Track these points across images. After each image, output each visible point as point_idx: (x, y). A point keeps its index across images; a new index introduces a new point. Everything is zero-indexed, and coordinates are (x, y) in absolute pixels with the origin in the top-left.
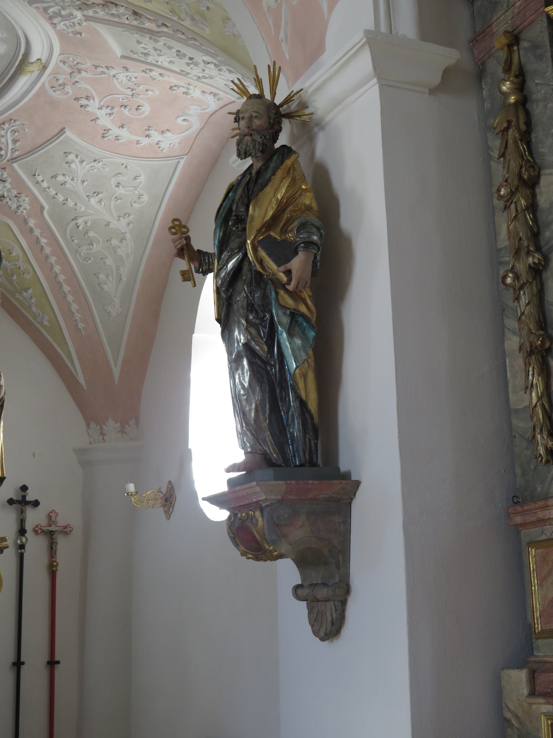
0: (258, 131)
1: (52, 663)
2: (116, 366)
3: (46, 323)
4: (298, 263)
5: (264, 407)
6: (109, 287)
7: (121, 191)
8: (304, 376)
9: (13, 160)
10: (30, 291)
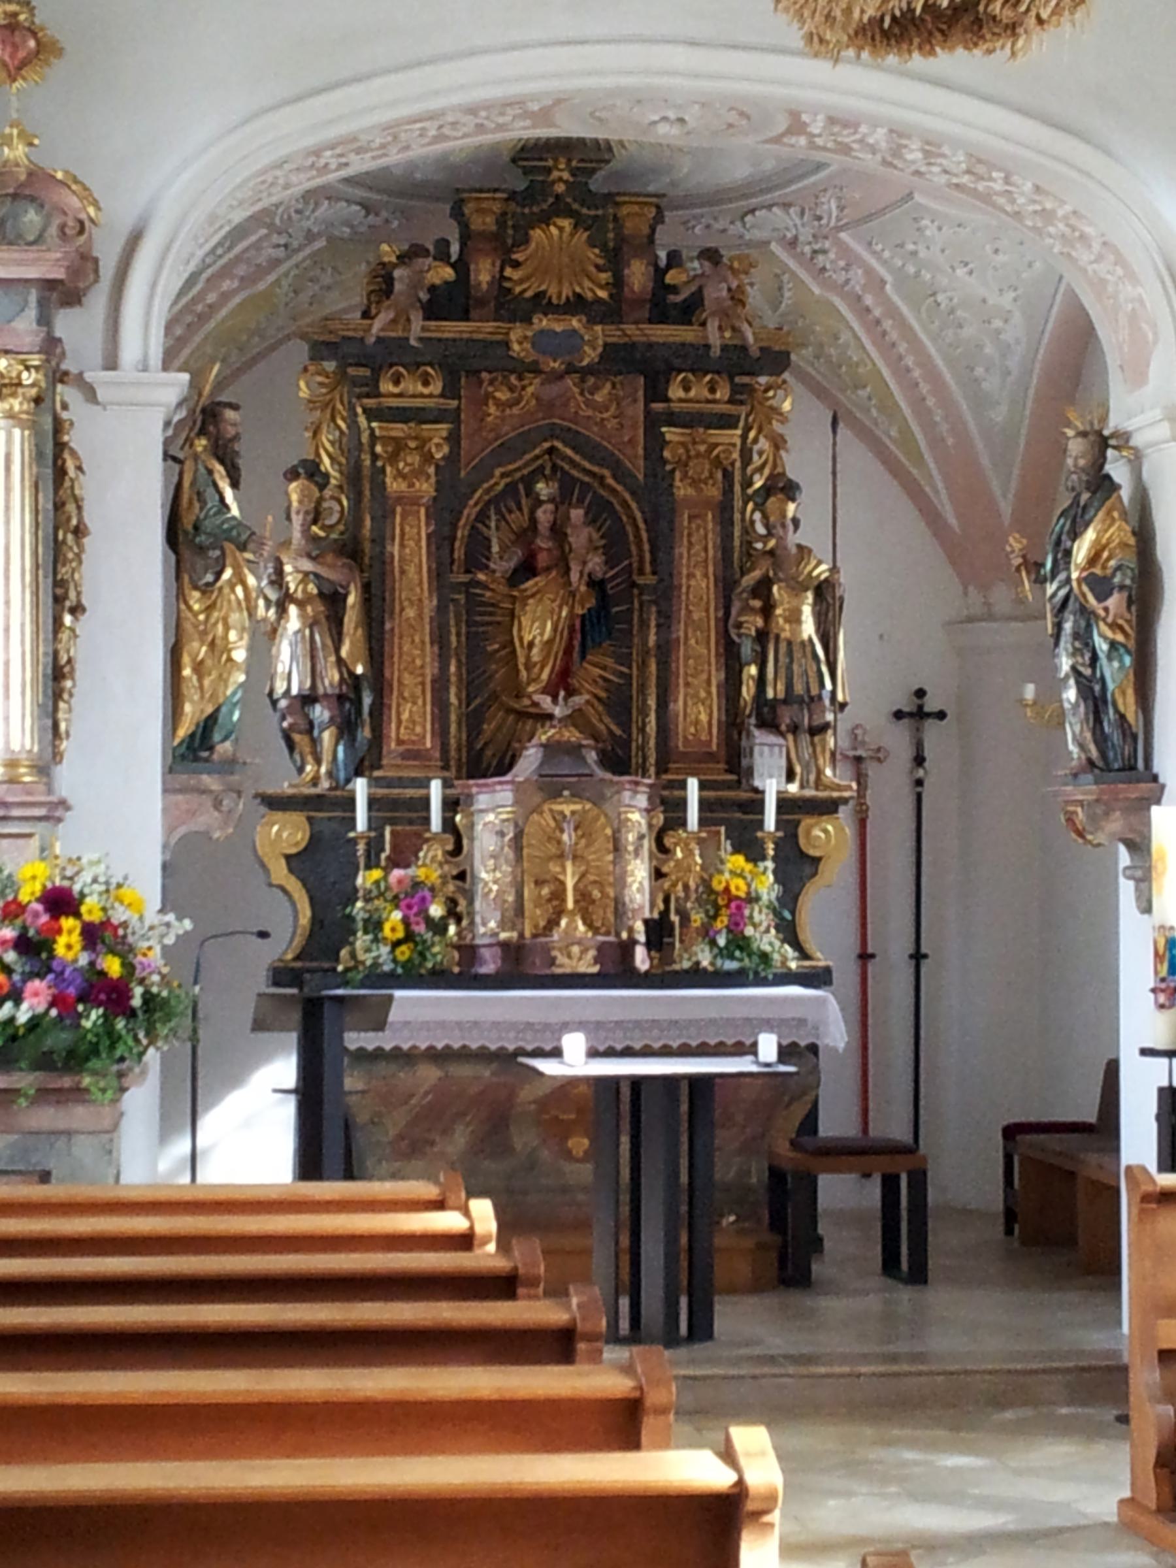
0: (1083, 470)
1: (918, 957)
2: (1004, 496)
3: (893, 433)
4: (1115, 601)
5: (1087, 720)
6: (991, 384)
7: (1001, 258)
8: (1124, 693)
9: (840, 229)
10: (868, 389)
